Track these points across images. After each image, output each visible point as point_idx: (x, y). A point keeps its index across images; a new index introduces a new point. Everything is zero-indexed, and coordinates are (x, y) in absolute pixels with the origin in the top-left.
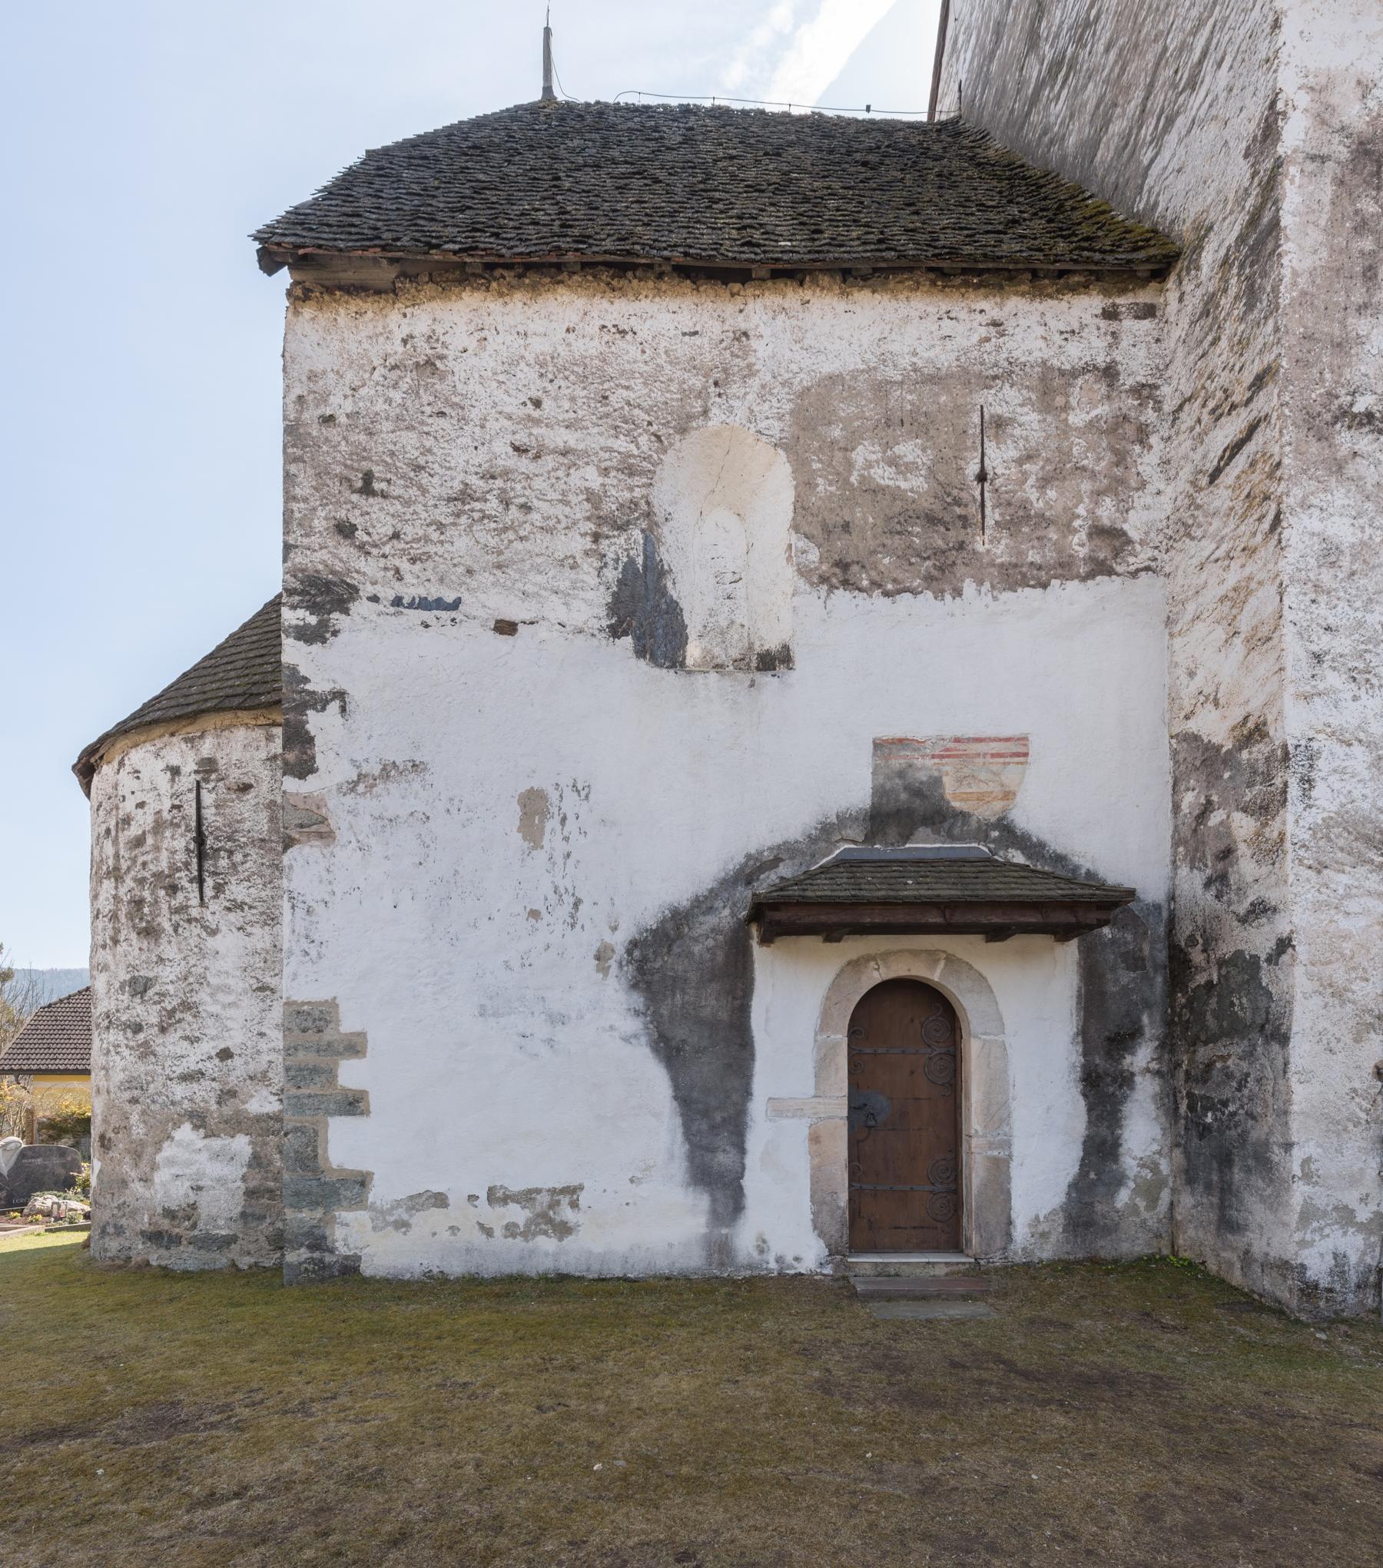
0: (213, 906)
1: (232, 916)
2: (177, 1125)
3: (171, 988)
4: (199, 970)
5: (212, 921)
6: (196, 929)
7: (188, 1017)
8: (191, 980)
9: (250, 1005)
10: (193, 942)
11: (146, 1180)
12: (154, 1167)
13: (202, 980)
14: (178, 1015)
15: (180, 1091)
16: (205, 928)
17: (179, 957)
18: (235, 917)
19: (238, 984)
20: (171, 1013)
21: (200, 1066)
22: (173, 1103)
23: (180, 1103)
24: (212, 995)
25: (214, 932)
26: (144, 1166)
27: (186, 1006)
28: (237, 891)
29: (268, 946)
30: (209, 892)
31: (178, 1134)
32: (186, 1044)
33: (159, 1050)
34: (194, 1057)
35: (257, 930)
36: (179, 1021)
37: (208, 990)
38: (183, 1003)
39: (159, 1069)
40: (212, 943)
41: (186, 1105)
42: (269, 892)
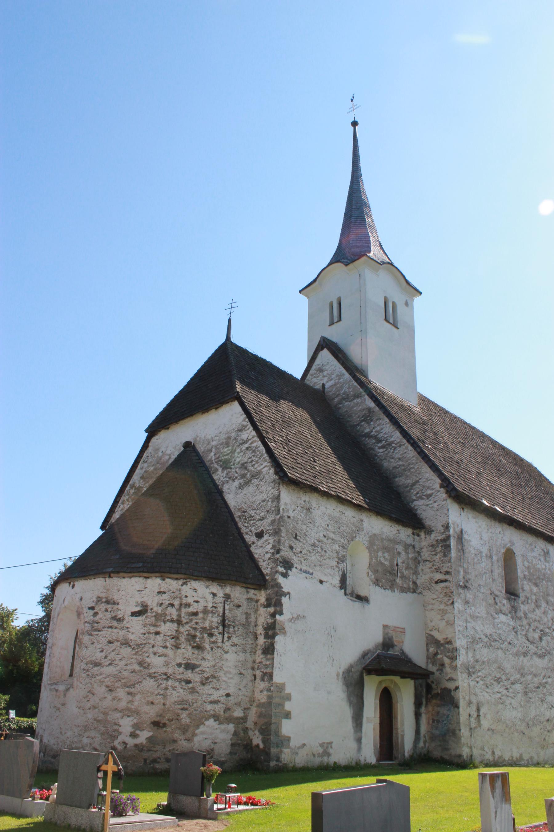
0: (227, 643)
1: (233, 648)
2: (207, 719)
3: (207, 670)
4: (220, 664)
5: (226, 648)
6: (220, 650)
7: (215, 681)
8: (216, 667)
9: (237, 679)
10: (218, 655)
11: (188, 740)
12: (194, 735)
13: (221, 668)
14: (210, 679)
15: (209, 707)
16: (224, 651)
17: (211, 659)
18: (234, 648)
19: (234, 671)
20: (207, 678)
21: (219, 698)
22: (206, 711)
23: (209, 711)
24: (225, 674)
25: (227, 652)
26: (188, 735)
27: (213, 677)
28: (235, 639)
29: (243, 659)
30: (226, 639)
31: (207, 723)
32: (213, 690)
33: (200, 691)
34: (216, 695)
35: (240, 654)
36: (211, 682)
37: (223, 672)
38: (212, 675)
39: (200, 698)
40: (226, 656)
41: (212, 712)
42: (245, 642)
